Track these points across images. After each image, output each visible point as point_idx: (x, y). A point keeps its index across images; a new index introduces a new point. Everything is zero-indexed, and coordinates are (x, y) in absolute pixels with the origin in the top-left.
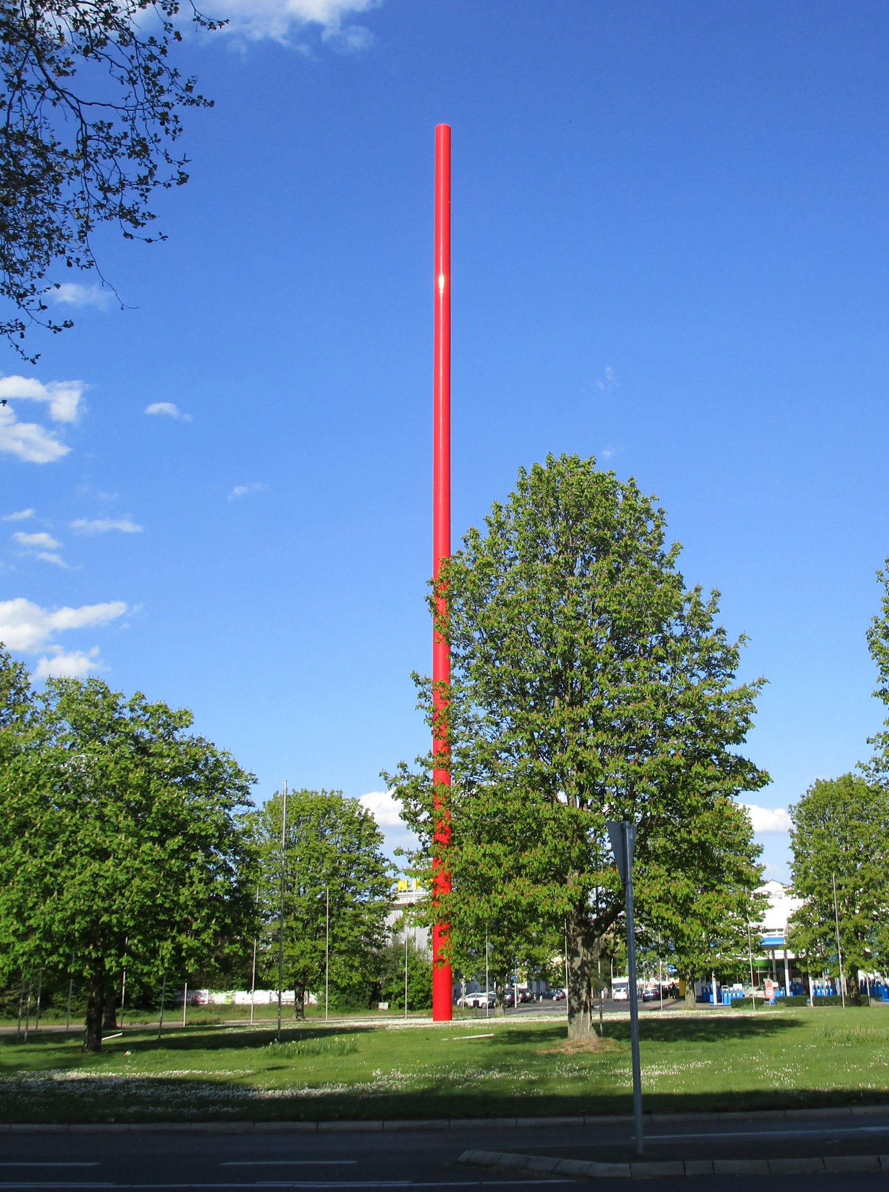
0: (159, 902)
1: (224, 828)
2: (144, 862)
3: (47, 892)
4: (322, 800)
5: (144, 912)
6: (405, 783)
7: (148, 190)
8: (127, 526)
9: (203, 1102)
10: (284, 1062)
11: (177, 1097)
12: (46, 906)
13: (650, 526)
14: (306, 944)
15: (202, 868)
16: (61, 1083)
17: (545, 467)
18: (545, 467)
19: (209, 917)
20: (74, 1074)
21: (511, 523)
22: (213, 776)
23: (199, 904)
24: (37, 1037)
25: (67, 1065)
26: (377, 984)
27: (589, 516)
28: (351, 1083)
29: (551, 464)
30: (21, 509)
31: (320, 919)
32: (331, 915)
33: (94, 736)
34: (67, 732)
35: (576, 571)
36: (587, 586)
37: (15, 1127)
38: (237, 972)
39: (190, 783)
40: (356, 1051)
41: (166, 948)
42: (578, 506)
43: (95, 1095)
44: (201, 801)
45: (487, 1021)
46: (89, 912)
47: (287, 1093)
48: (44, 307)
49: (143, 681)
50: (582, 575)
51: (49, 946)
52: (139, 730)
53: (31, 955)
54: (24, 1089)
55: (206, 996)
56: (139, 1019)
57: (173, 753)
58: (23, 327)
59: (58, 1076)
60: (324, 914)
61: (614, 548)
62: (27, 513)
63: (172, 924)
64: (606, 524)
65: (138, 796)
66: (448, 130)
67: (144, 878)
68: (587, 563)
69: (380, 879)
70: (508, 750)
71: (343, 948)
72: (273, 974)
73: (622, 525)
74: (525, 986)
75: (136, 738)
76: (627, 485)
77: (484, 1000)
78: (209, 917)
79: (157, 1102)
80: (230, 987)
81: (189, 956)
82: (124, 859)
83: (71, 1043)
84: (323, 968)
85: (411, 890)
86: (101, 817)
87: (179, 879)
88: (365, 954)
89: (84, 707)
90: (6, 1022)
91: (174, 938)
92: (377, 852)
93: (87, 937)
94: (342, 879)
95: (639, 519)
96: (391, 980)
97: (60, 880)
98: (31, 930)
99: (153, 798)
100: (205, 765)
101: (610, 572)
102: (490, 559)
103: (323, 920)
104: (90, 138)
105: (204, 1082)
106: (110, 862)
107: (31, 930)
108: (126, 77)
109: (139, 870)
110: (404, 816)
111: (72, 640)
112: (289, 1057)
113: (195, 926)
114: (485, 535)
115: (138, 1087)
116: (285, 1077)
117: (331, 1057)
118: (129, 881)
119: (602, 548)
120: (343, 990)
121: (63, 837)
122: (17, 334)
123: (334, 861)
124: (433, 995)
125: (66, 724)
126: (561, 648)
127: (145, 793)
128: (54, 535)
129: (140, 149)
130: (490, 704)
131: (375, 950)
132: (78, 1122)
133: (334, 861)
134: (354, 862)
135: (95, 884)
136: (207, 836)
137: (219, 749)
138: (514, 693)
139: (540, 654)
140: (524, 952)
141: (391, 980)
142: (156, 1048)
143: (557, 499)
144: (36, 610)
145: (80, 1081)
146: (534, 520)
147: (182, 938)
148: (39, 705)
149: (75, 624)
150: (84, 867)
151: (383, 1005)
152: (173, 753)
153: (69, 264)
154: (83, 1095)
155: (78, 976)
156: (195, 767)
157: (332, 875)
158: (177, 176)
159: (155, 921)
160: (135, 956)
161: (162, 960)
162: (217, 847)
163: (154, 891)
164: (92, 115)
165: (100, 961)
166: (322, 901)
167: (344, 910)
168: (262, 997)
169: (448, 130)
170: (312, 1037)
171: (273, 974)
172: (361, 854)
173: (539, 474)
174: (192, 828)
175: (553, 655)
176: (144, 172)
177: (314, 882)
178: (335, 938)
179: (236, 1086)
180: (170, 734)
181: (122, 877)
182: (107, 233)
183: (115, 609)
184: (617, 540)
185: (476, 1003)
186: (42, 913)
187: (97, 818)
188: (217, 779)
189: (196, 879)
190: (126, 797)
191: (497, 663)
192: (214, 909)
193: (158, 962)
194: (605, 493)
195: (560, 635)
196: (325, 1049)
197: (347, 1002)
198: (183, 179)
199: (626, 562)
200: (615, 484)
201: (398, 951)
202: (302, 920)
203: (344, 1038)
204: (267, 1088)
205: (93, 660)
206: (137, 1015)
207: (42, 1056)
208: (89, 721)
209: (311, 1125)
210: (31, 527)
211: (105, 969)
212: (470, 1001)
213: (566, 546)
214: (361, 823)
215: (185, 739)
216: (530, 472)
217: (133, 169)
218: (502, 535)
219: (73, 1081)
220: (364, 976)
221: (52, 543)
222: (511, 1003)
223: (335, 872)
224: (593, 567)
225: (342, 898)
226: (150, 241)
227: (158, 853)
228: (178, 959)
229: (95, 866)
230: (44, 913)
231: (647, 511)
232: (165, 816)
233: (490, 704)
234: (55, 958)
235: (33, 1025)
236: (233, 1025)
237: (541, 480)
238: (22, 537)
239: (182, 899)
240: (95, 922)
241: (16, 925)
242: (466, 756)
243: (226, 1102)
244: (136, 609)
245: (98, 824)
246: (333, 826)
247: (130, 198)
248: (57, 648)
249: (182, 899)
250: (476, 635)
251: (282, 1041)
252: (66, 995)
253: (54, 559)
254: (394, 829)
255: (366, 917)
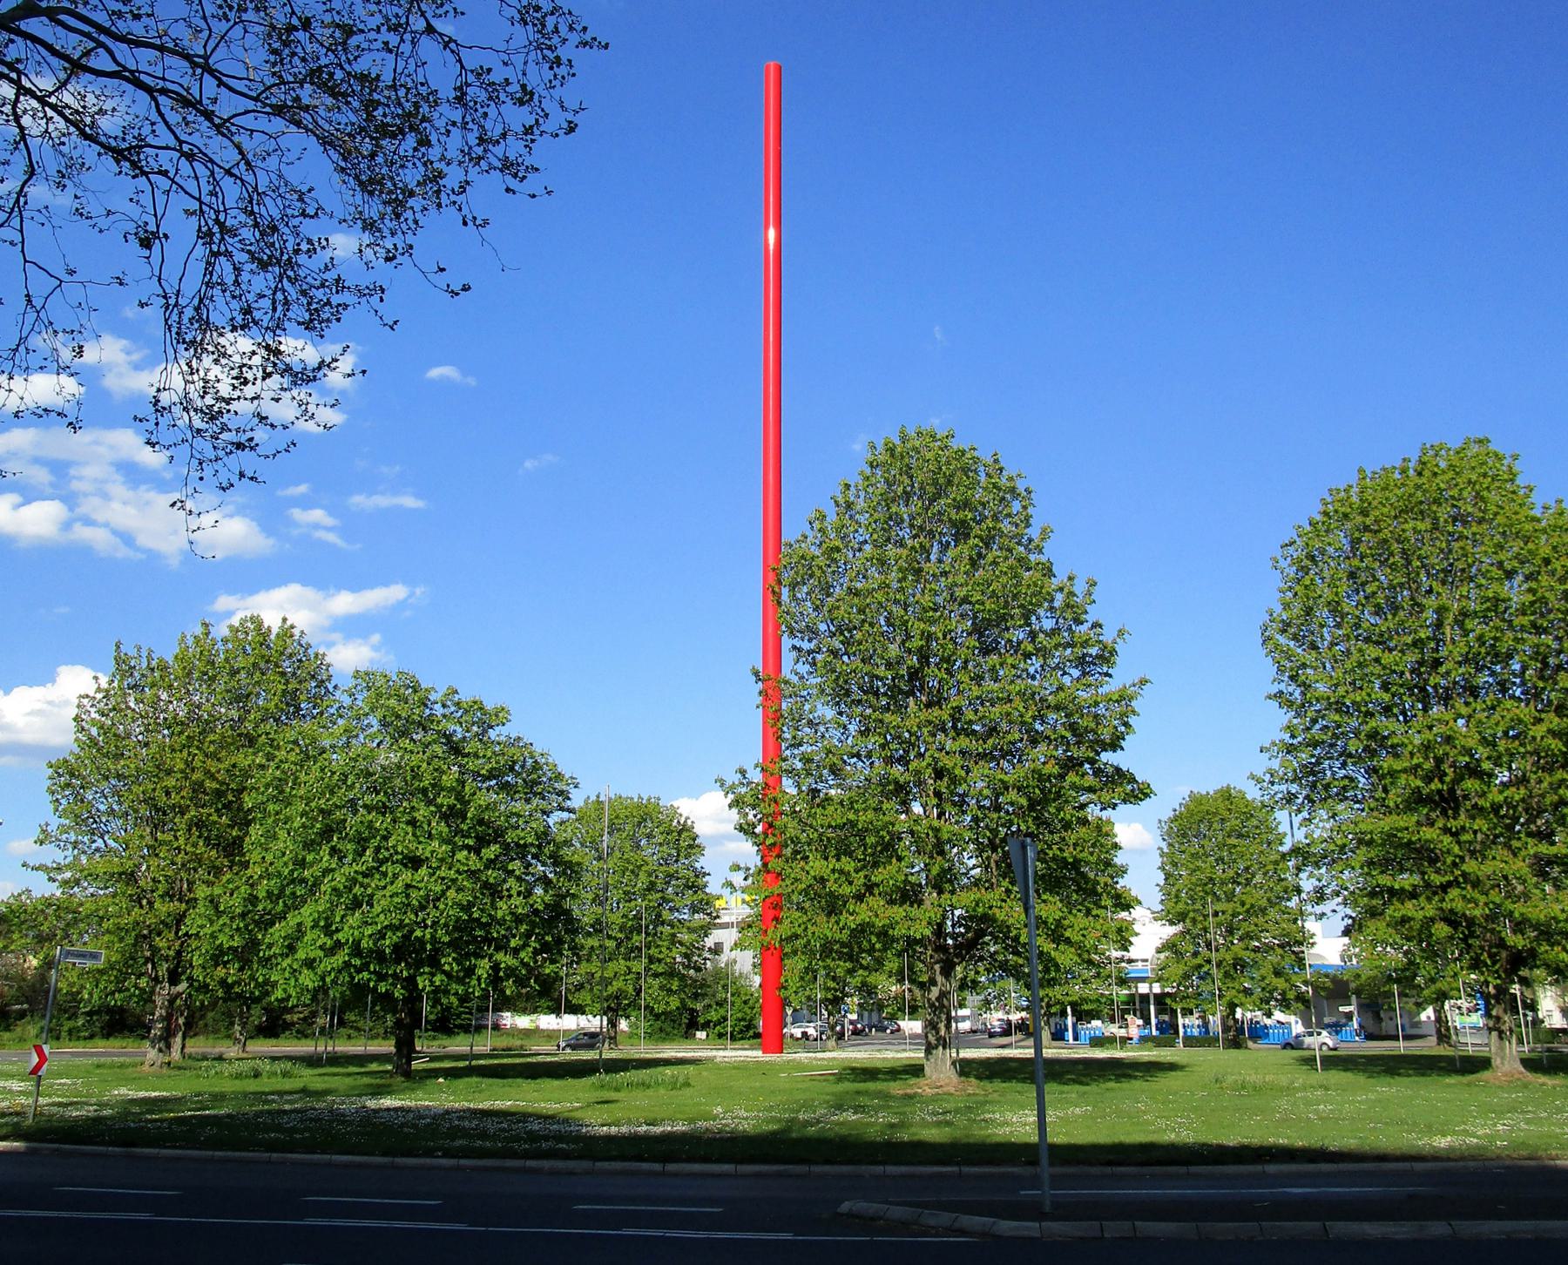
0: (476, 915)
1: (544, 836)
2: (458, 872)
3: (356, 904)
4: (639, 806)
5: (460, 927)
6: (743, 790)
7: (533, 141)
8: (409, 502)
9: (533, 1137)
10: (613, 1095)
11: (503, 1130)
12: (355, 919)
13: (1016, 506)
14: (620, 965)
15: (519, 879)
16: (376, 1111)
17: (897, 442)
18: (897, 442)
19: (528, 935)
20: (388, 1102)
21: (861, 504)
22: (530, 778)
23: (518, 919)
24: (335, 1060)
25: (378, 1092)
26: (693, 1011)
27: (947, 496)
28: (692, 1121)
29: (904, 439)
30: (297, 485)
31: (635, 938)
32: (647, 934)
33: (404, 733)
34: (375, 729)
35: (933, 557)
36: (945, 574)
37: (334, 1157)
38: (550, 997)
39: (505, 787)
40: (688, 1085)
41: (483, 967)
42: (935, 483)
43: (415, 1126)
44: (518, 806)
45: (820, 1055)
46: (401, 926)
47: (624, 1129)
48: (442, 270)
49: (454, 673)
50: (940, 561)
51: (358, 962)
52: (451, 727)
53: (340, 971)
54: (338, 1117)
55: (508, 1019)
56: (436, 1043)
57: (489, 754)
58: (383, 291)
59: (372, 1104)
60: (639, 933)
61: (976, 531)
62: (303, 488)
63: (488, 940)
64: (966, 505)
65: (452, 801)
66: (779, 69)
67: (459, 890)
68: (945, 547)
69: (700, 895)
70: (858, 756)
71: (660, 970)
72: (583, 997)
73: (983, 504)
74: (854, 1017)
75: (448, 737)
76: (990, 461)
77: (811, 1032)
78: (528, 935)
79: (484, 1135)
80: (534, 1011)
81: (508, 977)
82: (439, 868)
83: (374, 1067)
84: (638, 992)
85: (735, 908)
86: (413, 822)
87: (494, 891)
88: (683, 978)
89: (392, 702)
90: (295, 1041)
91: (491, 957)
92: (697, 865)
93: (400, 952)
94: (659, 895)
95: (1003, 499)
96: (710, 1006)
97: (369, 891)
98: (338, 945)
99: (469, 802)
100: (523, 767)
101: (971, 558)
102: (838, 543)
103: (637, 939)
104: (468, 85)
105: (530, 1115)
106: (423, 871)
107: (338, 945)
108: (517, 17)
109: (454, 881)
110: (741, 829)
111: (352, 627)
112: (617, 1090)
113: (513, 943)
114: (832, 518)
115: (459, 1118)
116: (617, 1112)
117: (662, 1091)
118: (444, 893)
119: (961, 531)
120: (657, 1017)
121: (375, 843)
122: (377, 298)
123: (650, 875)
124: (756, 1026)
125: (373, 720)
126: (916, 643)
127: (460, 797)
128: (331, 511)
129: (525, 97)
130: (838, 704)
131: (692, 972)
132: (403, 1155)
133: (650, 875)
134: (671, 876)
135: (408, 896)
136: (525, 845)
137: (537, 749)
138: (865, 693)
139: (894, 650)
140: (859, 979)
141: (710, 1006)
142: (467, 1076)
143: (911, 477)
144: (310, 593)
145: (396, 1109)
146: (888, 501)
147: (500, 956)
148: (347, 701)
149: (354, 609)
150: (396, 876)
151: (701, 1035)
152: (489, 754)
153: (465, 223)
154: (402, 1125)
155: (388, 996)
156: (512, 769)
157: (648, 889)
158: (565, 125)
159: (470, 937)
160: (448, 975)
161: (479, 979)
162: (535, 856)
163: (471, 905)
164: (472, 60)
165: (411, 981)
166: (638, 917)
167: (660, 929)
168: (570, 1022)
169: (779, 69)
170: (625, 1069)
171: (583, 997)
172: (678, 867)
173: (891, 451)
174: (510, 837)
175: (909, 651)
176: (530, 121)
177: (629, 897)
178: (651, 960)
179: (566, 1121)
180: (485, 732)
181: (438, 889)
182: (486, 189)
183: (396, 592)
184: (979, 523)
185: (805, 1034)
186: (351, 927)
187: (408, 823)
188: (536, 783)
189: (514, 892)
190: (439, 800)
191: (845, 658)
192: (533, 925)
193: (474, 982)
194: (965, 470)
195: (917, 627)
196: (657, 1083)
197: (661, 1030)
198: (571, 129)
199: (987, 545)
200: (976, 460)
201: (719, 975)
202: (615, 939)
203: (668, 1071)
204: (599, 1123)
205: (375, 648)
206: (434, 1038)
207: (348, 1081)
208: (398, 717)
209: (657, 1167)
210: (306, 503)
211: (409, 989)
212: (798, 1033)
213: (921, 528)
214: (680, 833)
215: (503, 738)
216: (881, 448)
217: (517, 117)
218: (851, 517)
219: (388, 1109)
220: (682, 1001)
221: (329, 521)
222: (841, 1036)
223: (651, 887)
224: (951, 553)
225: (659, 915)
226: (534, 196)
227: (474, 863)
228: (495, 979)
229: (407, 876)
230: (351, 927)
231: (1013, 490)
232: (481, 822)
233: (838, 704)
234: (365, 975)
235: (322, 1047)
236: (544, 1052)
237: (892, 456)
238: (297, 514)
239: (500, 914)
240: (406, 937)
241: (323, 939)
242: (810, 761)
243: (559, 1137)
244: (418, 591)
245: (410, 829)
246: (649, 836)
247: (514, 148)
248: (336, 636)
249: (500, 914)
250: (823, 627)
251: (607, 1072)
252: (362, 1014)
253: (331, 537)
254: (720, 839)
255: (685, 937)
